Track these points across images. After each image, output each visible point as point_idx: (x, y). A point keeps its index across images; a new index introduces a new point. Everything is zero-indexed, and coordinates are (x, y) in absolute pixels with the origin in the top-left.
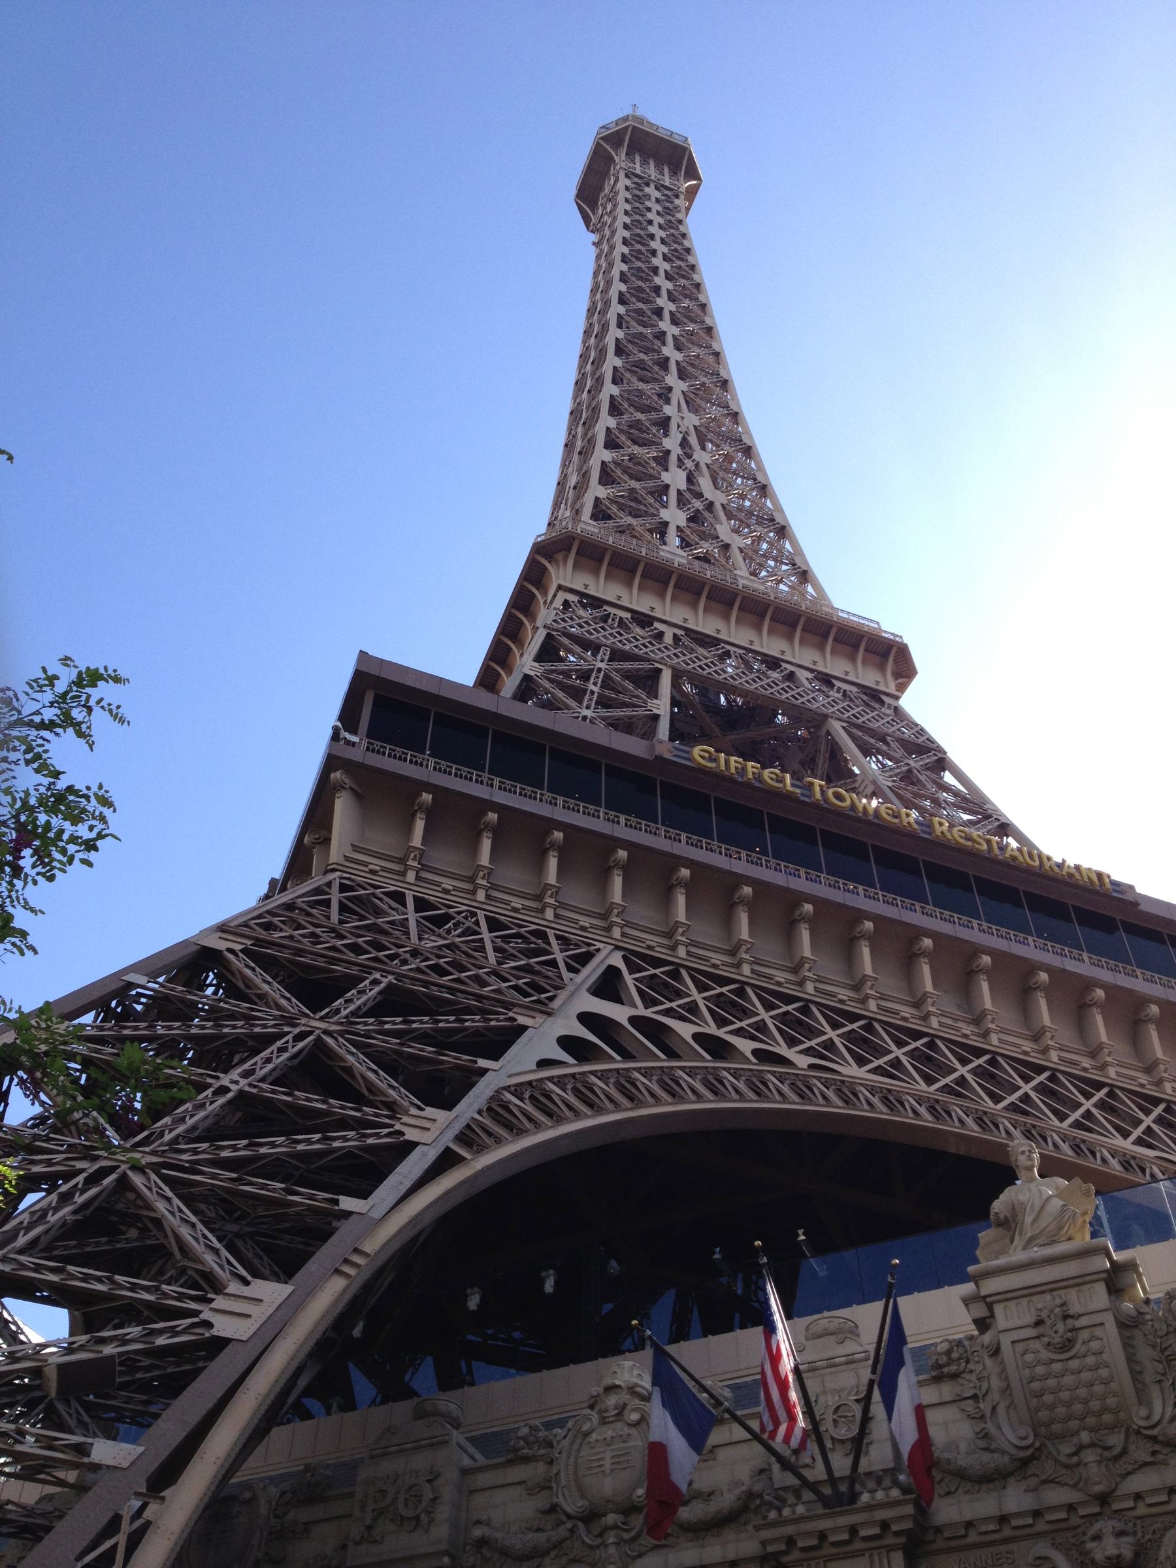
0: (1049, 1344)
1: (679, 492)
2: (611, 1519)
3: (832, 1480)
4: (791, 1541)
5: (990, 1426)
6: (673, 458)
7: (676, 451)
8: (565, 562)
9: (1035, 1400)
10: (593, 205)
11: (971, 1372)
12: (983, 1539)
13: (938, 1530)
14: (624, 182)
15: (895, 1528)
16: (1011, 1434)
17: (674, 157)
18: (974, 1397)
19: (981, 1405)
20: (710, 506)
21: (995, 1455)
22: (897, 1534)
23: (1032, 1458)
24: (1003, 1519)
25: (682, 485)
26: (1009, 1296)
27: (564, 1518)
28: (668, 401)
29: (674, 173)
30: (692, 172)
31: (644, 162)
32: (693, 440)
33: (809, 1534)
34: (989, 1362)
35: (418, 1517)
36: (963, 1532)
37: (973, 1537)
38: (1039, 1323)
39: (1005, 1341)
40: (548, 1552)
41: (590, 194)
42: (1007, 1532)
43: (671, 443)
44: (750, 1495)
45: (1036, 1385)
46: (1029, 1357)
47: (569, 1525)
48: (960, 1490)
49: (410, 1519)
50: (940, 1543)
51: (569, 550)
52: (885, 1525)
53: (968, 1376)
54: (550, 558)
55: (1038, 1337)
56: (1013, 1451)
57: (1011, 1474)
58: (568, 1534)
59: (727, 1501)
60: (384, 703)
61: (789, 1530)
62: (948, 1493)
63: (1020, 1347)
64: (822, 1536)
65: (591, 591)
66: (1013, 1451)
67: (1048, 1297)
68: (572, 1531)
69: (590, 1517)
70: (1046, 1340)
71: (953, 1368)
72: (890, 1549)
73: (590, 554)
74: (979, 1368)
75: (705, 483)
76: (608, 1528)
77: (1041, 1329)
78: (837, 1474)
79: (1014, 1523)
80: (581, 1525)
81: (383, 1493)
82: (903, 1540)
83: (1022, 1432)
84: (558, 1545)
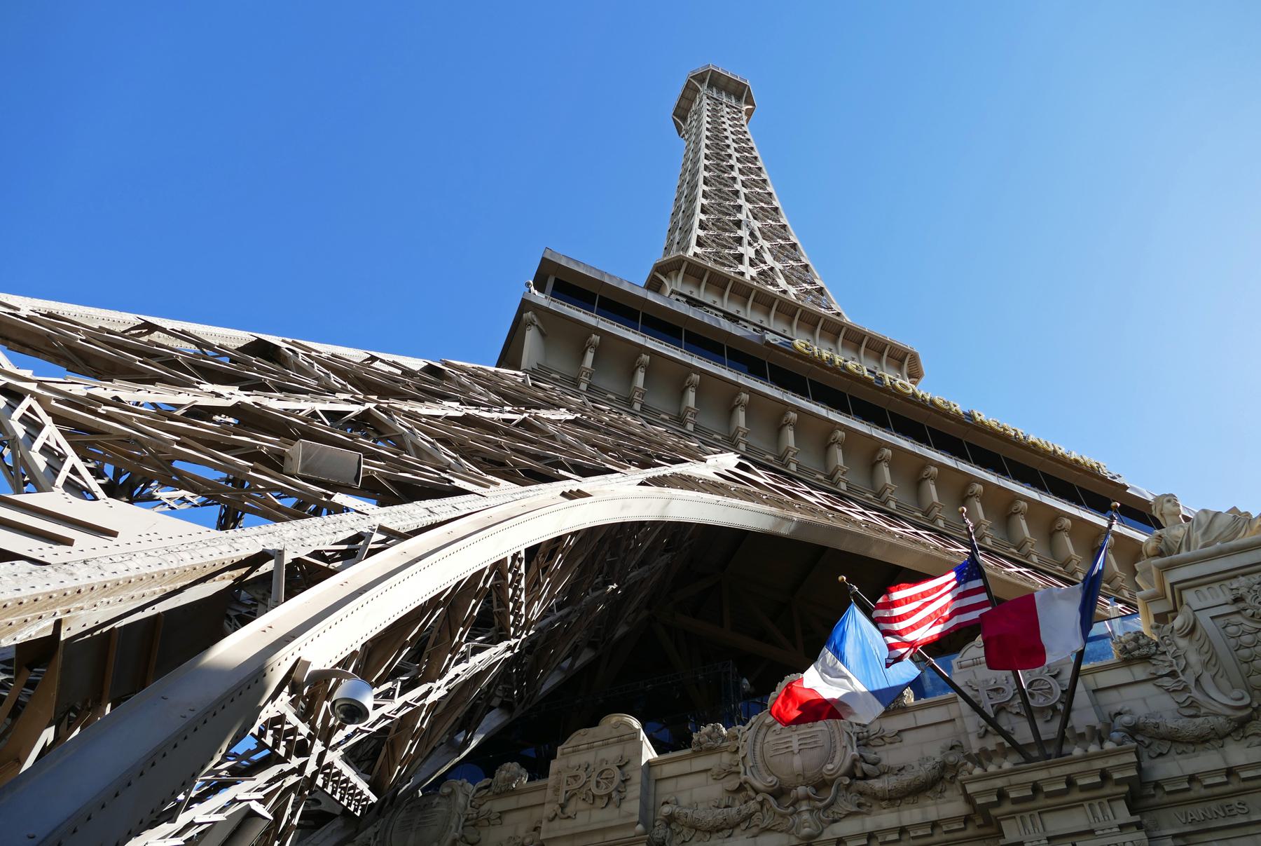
0: (1253, 616)
1: (751, 259)
2: (801, 790)
3: (1039, 742)
4: (1002, 795)
5: (1196, 694)
6: (745, 241)
7: (747, 238)
8: (677, 276)
9: (1245, 666)
10: (684, 119)
11: (1164, 653)
12: (1209, 792)
13: (1158, 785)
14: (705, 101)
15: (1116, 776)
16: (1223, 699)
17: (739, 92)
18: (1173, 674)
19: (1182, 678)
20: (772, 269)
21: (1210, 718)
22: (1119, 782)
23: (1249, 719)
24: (1230, 772)
25: (753, 256)
26: (1196, 583)
27: (752, 794)
28: (740, 212)
29: (739, 99)
30: (749, 101)
31: (719, 92)
32: (758, 234)
33: (1021, 785)
34: (1182, 643)
35: (609, 796)
36: (1186, 785)
37: (1197, 790)
38: (1237, 600)
39: (1204, 619)
40: (738, 825)
41: (682, 113)
42: (1235, 785)
43: (743, 233)
44: (944, 767)
45: (1245, 653)
46: (1231, 629)
47: (759, 798)
48: (1173, 751)
49: (601, 797)
50: (1160, 798)
51: (679, 270)
52: (1105, 775)
53: (1161, 658)
54: (666, 275)
55: (1238, 612)
56: (1229, 712)
57: (1228, 735)
58: (758, 807)
59: (922, 772)
60: (560, 281)
61: (999, 783)
62: (1161, 755)
63: (1221, 622)
64: (1036, 788)
65: (695, 296)
66: (1229, 712)
67: (1241, 579)
68: (762, 804)
69: (779, 793)
70: (1250, 612)
71: (1144, 651)
72: (1112, 799)
73: (695, 272)
74: (1172, 649)
75: (768, 257)
76: (797, 801)
77: (1241, 605)
78: (1043, 738)
79: (1244, 775)
80: (771, 799)
81: (575, 777)
82: (1126, 788)
83: (1237, 693)
84: (749, 816)
